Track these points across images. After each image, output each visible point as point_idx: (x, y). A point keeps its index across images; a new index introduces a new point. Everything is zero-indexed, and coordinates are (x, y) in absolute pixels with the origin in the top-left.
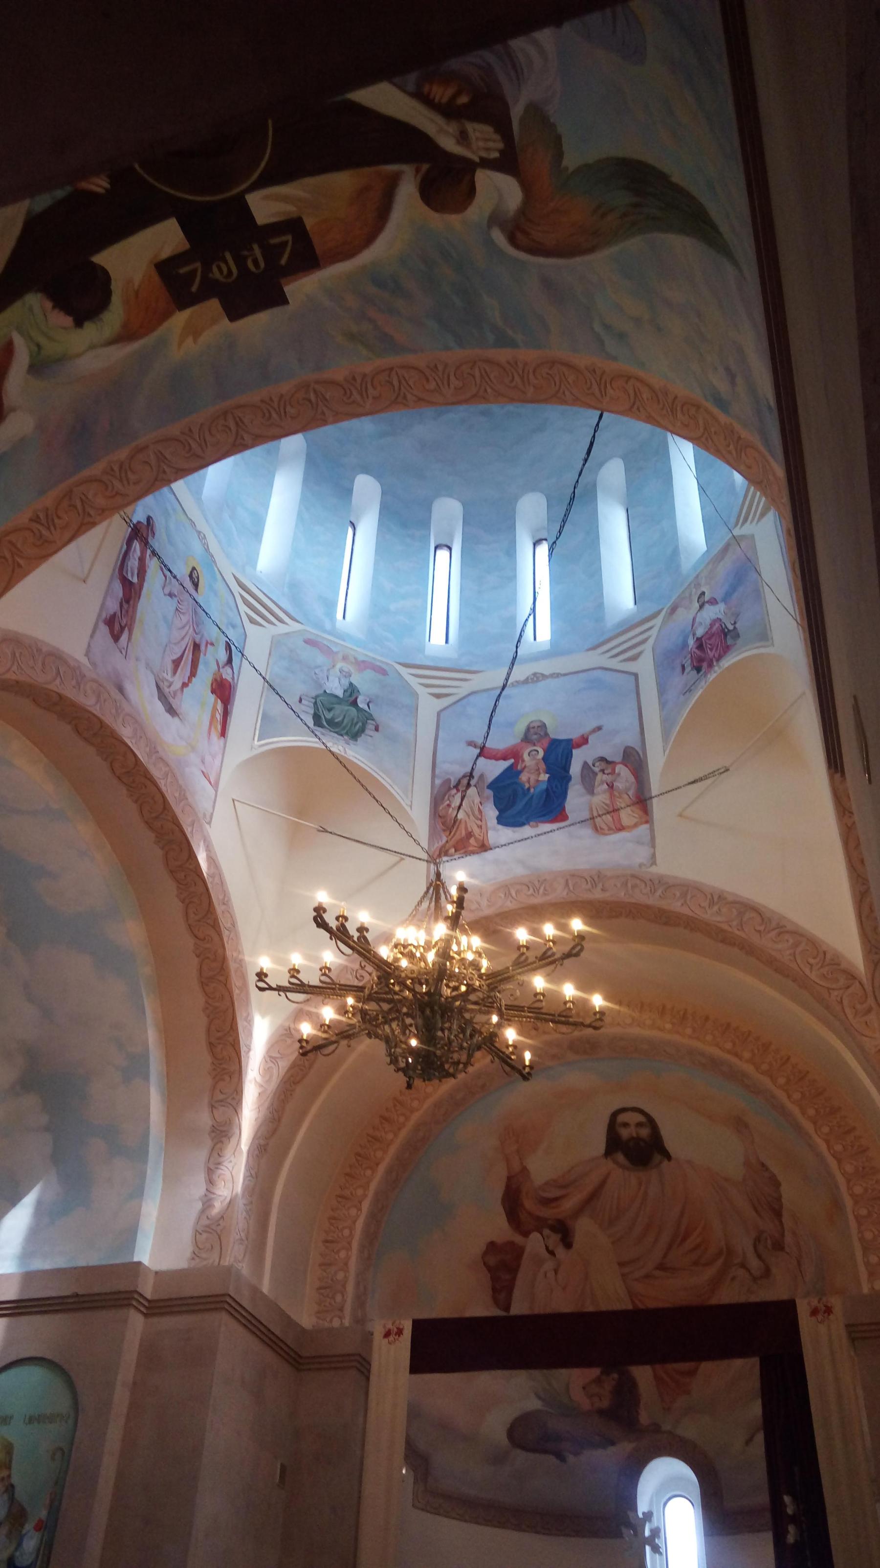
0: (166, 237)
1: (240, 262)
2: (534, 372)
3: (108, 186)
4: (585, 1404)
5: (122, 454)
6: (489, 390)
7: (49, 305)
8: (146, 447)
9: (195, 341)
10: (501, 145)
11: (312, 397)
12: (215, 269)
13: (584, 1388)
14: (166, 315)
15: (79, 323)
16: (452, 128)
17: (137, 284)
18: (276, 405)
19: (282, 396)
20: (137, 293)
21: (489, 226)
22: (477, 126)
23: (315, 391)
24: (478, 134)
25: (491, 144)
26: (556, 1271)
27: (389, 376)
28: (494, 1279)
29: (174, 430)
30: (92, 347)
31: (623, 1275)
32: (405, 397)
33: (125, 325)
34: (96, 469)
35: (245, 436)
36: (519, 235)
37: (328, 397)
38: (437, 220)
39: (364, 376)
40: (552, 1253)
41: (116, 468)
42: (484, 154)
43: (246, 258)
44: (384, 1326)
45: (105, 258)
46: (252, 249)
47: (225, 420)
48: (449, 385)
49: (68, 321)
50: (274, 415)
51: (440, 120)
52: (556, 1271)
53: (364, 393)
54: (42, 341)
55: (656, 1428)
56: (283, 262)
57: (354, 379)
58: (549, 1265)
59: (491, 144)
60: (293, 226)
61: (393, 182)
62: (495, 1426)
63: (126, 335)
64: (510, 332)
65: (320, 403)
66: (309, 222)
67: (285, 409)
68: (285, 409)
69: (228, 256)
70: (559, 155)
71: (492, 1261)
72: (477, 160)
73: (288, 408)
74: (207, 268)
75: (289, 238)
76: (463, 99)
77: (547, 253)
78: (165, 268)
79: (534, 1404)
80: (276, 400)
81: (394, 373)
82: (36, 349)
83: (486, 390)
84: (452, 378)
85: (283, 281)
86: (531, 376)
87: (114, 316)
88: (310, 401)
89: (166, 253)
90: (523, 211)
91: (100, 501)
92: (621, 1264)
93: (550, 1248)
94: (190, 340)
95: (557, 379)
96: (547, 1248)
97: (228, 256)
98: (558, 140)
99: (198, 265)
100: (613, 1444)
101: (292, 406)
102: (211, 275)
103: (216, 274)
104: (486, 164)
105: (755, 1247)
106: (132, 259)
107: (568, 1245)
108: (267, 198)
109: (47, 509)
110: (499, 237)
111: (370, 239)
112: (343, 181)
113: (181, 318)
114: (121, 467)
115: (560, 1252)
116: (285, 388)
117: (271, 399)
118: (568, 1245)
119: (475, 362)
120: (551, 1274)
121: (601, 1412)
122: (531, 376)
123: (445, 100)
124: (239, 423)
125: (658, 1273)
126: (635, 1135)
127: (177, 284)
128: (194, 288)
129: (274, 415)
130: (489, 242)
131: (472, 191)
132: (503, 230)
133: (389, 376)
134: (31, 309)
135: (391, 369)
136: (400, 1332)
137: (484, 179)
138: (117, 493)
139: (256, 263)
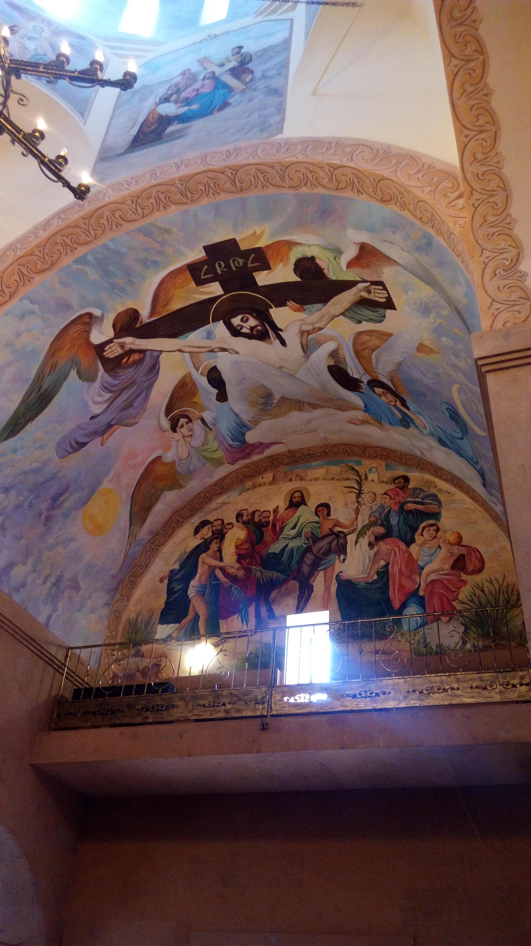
0: (263, 279)
1: (228, 266)
2: (60, 252)
3: (287, 302)
5: (304, 190)
6: (83, 226)
7: (325, 271)
8: (289, 187)
9: (255, 233)
10: (105, 354)
11: (189, 195)
12: (241, 264)
14: (269, 247)
15: (313, 258)
16: (127, 347)
17: (281, 264)
18: (211, 191)
19: (207, 196)
20: (282, 260)
21: (103, 316)
22: (117, 354)
23: (187, 198)
24: (116, 351)
25: (109, 351)
27: (143, 212)
29: (271, 190)
30: (310, 246)
32: (132, 201)
33: (290, 249)
34: (320, 190)
35: (230, 175)
36: (87, 320)
37: (180, 195)
38: (130, 304)
39: (158, 210)
41: (309, 185)
42: (112, 345)
43: (224, 268)
45: (295, 278)
46: (221, 271)
47: (241, 186)
48: (107, 218)
49: (317, 261)
50: (212, 185)
51: (134, 347)
53: (157, 199)
54: (333, 260)
56: (206, 267)
57: (164, 207)
59: (109, 351)
60: (200, 282)
61: (152, 314)
63: (291, 244)
64: (80, 267)
65: (184, 191)
66: (193, 284)
67: (205, 189)
68: (205, 189)
69: (234, 269)
70: (79, 373)
72: (114, 340)
73: (203, 189)
74: (245, 264)
75: (202, 277)
76: (124, 361)
77: (73, 322)
78: (266, 266)
80: (211, 194)
81: (141, 214)
82: (336, 258)
83: (85, 224)
84: (106, 224)
85: (206, 258)
86: (61, 249)
87: (295, 254)
88: (190, 192)
89: (265, 272)
90: (88, 332)
91: (322, 174)
94: (258, 233)
95: (46, 257)
97: (234, 269)
98: (80, 378)
99: (249, 266)
101: (201, 190)
102: (243, 261)
103: (241, 261)
104: (110, 341)
106: (282, 273)
108: (213, 293)
109: (352, 190)
110: (97, 312)
111: (162, 283)
112: (176, 305)
113: (261, 244)
114: (306, 183)
116: (205, 201)
117: (214, 195)
119: (95, 239)
122: (61, 249)
123: (133, 356)
124: (234, 183)
127: (261, 258)
128: (253, 256)
129: (212, 185)
130: (101, 306)
131: (114, 326)
132: (96, 317)
133: (143, 212)
134: (334, 274)
135: (143, 217)
137: (111, 334)
138: (311, 172)
139: (220, 266)
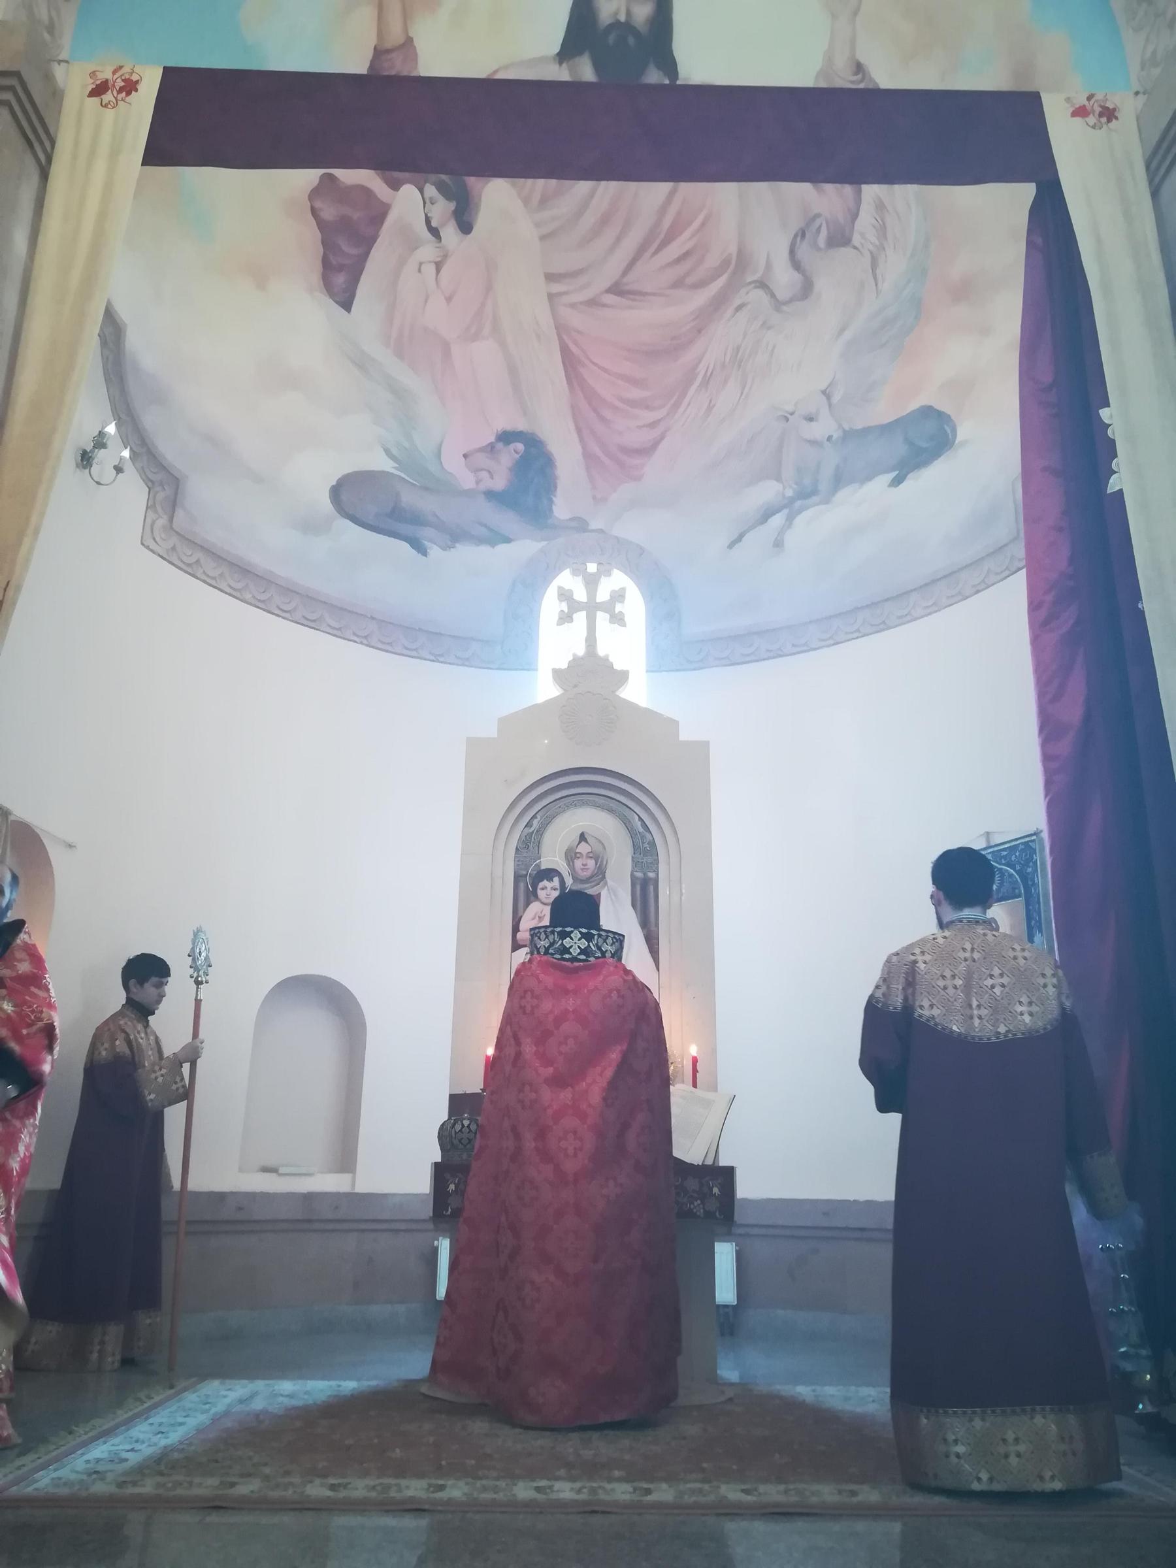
4: (467, 480)
13: (465, 456)
26: (439, 266)
28: (327, 244)
31: (551, 296)
40: (435, 232)
44: (93, 74)
52: (439, 266)
55: (580, 525)
58: (428, 252)
62: (314, 475)
71: (329, 212)
79: (382, 463)
92: (550, 277)
93: (434, 224)
96: (428, 221)
100: (508, 540)
105: (792, 252)
107: (466, 227)
115: (450, 233)
118: (466, 227)
120: (430, 270)
121: (490, 495)
125: (610, 299)
126: (622, 18)
136: (130, 87)
